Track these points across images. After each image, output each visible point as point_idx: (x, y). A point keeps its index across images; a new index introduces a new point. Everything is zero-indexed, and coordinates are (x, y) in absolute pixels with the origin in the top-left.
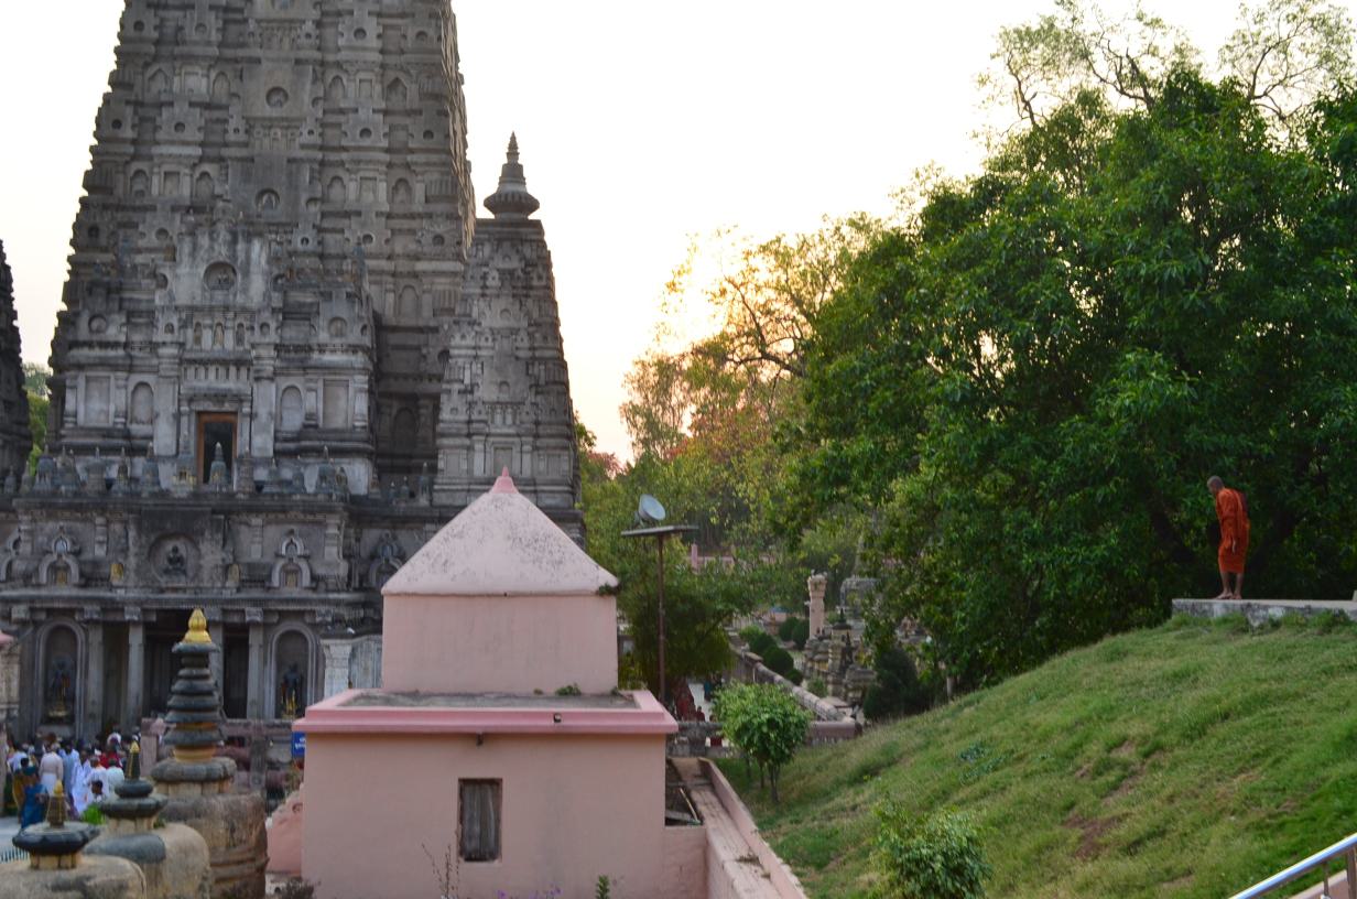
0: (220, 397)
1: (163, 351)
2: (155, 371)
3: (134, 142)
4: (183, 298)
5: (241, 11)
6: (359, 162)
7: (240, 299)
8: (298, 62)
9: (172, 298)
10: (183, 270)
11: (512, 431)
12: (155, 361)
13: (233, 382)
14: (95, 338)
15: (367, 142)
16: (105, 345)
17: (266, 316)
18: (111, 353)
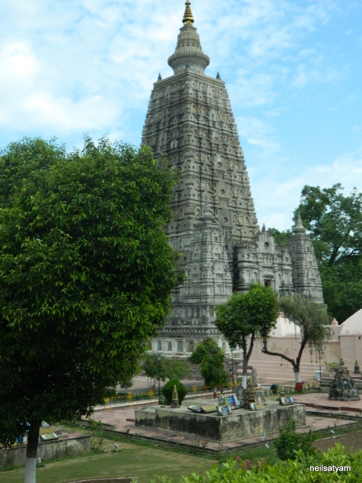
0: (268, 276)
1: (260, 264)
2: (258, 269)
3: (197, 201)
4: (262, 252)
5: (211, 166)
6: (240, 212)
7: (271, 252)
8: (226, 183)
9: (259, 250)
10: (261, 243)
11: (314, 285)
12: (258, 267)
13: (270, 273)
14: (248, 260)
15: (241, 207)
16: (250, 262)
17: (276, 257)
18: (251, 264)
